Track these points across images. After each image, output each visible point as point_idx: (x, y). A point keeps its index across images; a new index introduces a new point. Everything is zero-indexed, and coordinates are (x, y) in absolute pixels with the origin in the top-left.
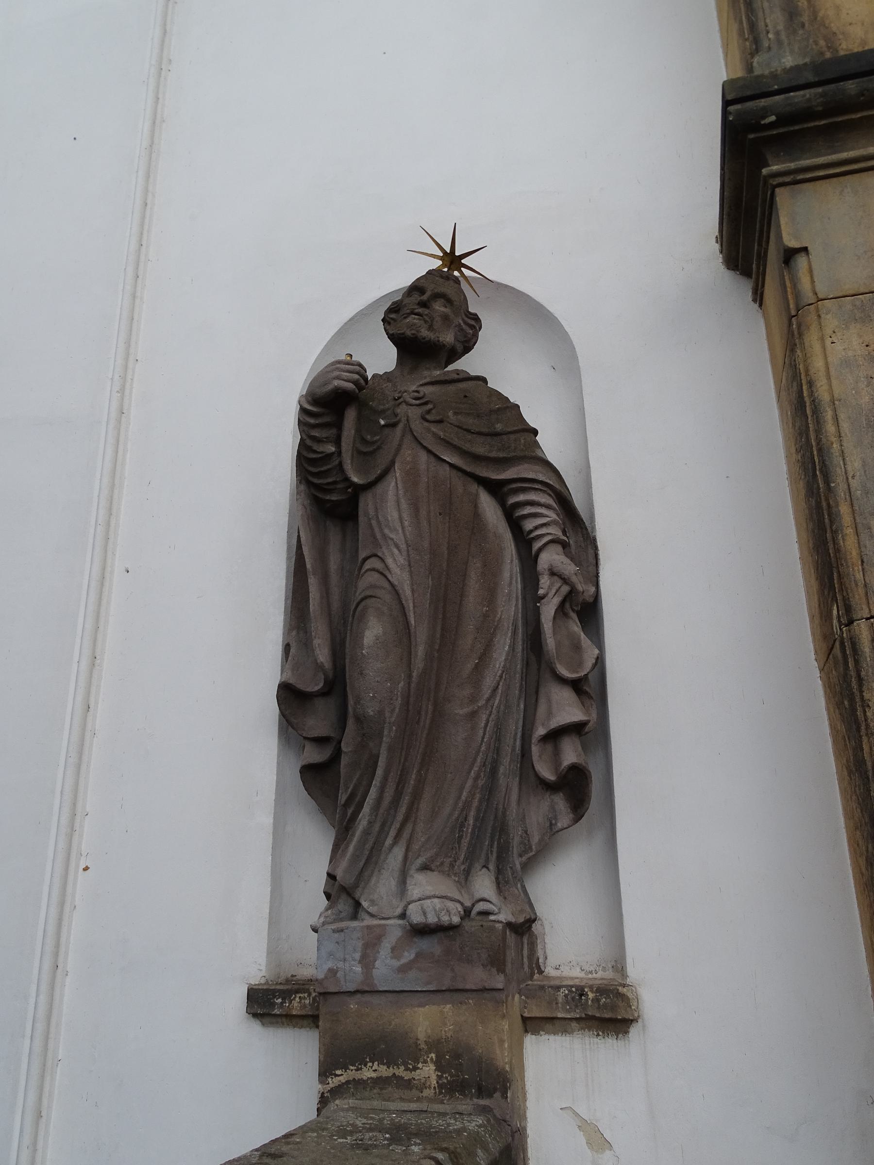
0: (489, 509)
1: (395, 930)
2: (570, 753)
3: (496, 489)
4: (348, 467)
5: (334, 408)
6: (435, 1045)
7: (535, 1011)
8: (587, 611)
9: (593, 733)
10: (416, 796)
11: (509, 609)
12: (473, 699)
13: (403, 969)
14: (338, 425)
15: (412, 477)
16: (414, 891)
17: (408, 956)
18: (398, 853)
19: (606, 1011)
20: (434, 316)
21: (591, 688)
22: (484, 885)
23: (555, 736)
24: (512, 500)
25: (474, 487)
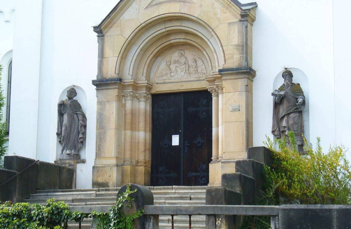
0: (75, 116)
1: (65, 154)
2: (81, 140)
3: (77, 114)
4: (62, 111)
5: (62, 106)
6: (68, 163)
7: (78, 162)
8: (85, 127)
9: (84, 138)
10: (68, 144)
11: (76, 126)
12: (73, 134)
13: (66, 157)
14: (61, 106)
15: (68, 112)
16: (67, 151)
17: (66, 156)
18: (66, 148)
19: (84, 162)
20: (72, 92)
21: (84, 134)
22: (73, 151)
23: (80, 138)
24: (78, 115)
25: (74, 114)
